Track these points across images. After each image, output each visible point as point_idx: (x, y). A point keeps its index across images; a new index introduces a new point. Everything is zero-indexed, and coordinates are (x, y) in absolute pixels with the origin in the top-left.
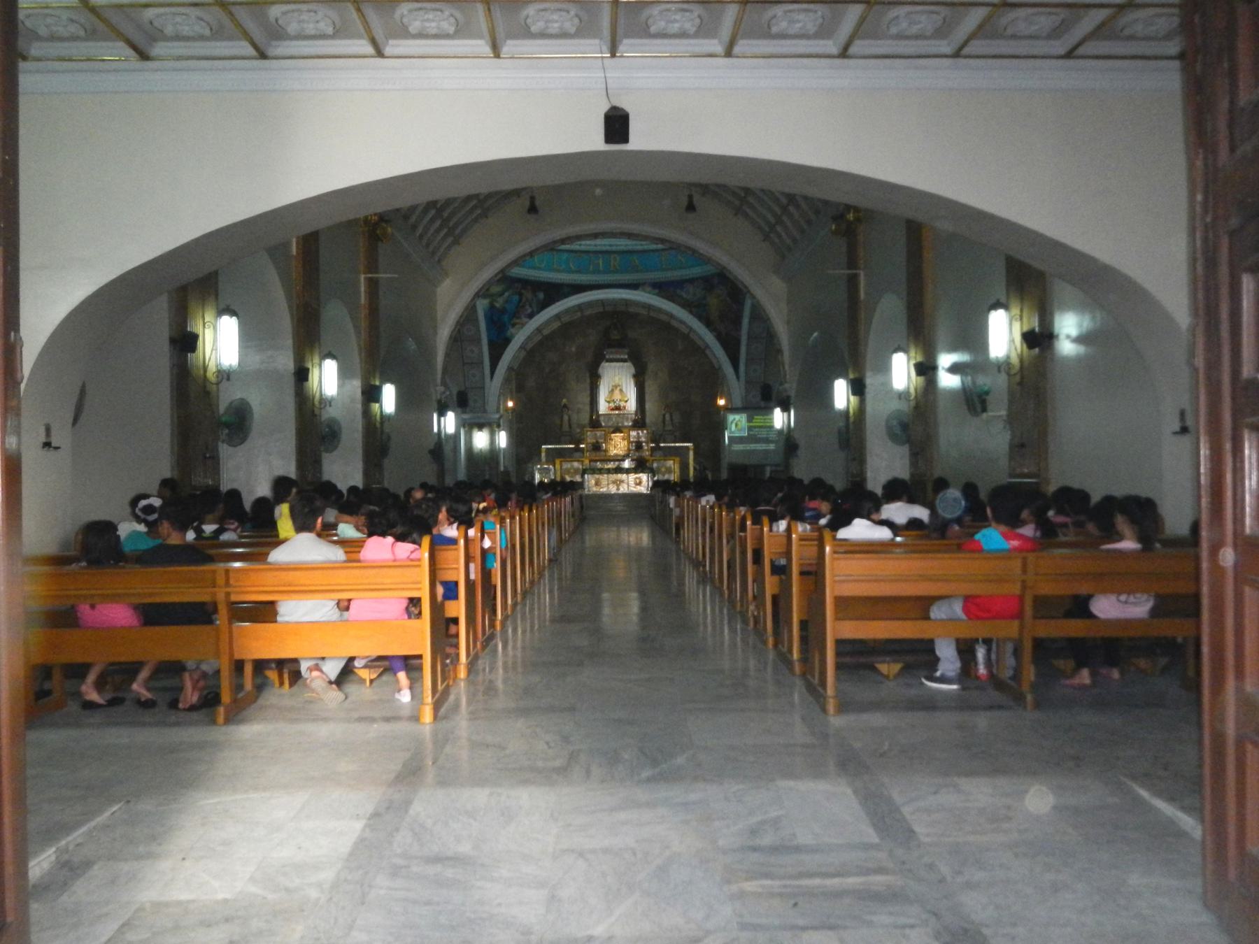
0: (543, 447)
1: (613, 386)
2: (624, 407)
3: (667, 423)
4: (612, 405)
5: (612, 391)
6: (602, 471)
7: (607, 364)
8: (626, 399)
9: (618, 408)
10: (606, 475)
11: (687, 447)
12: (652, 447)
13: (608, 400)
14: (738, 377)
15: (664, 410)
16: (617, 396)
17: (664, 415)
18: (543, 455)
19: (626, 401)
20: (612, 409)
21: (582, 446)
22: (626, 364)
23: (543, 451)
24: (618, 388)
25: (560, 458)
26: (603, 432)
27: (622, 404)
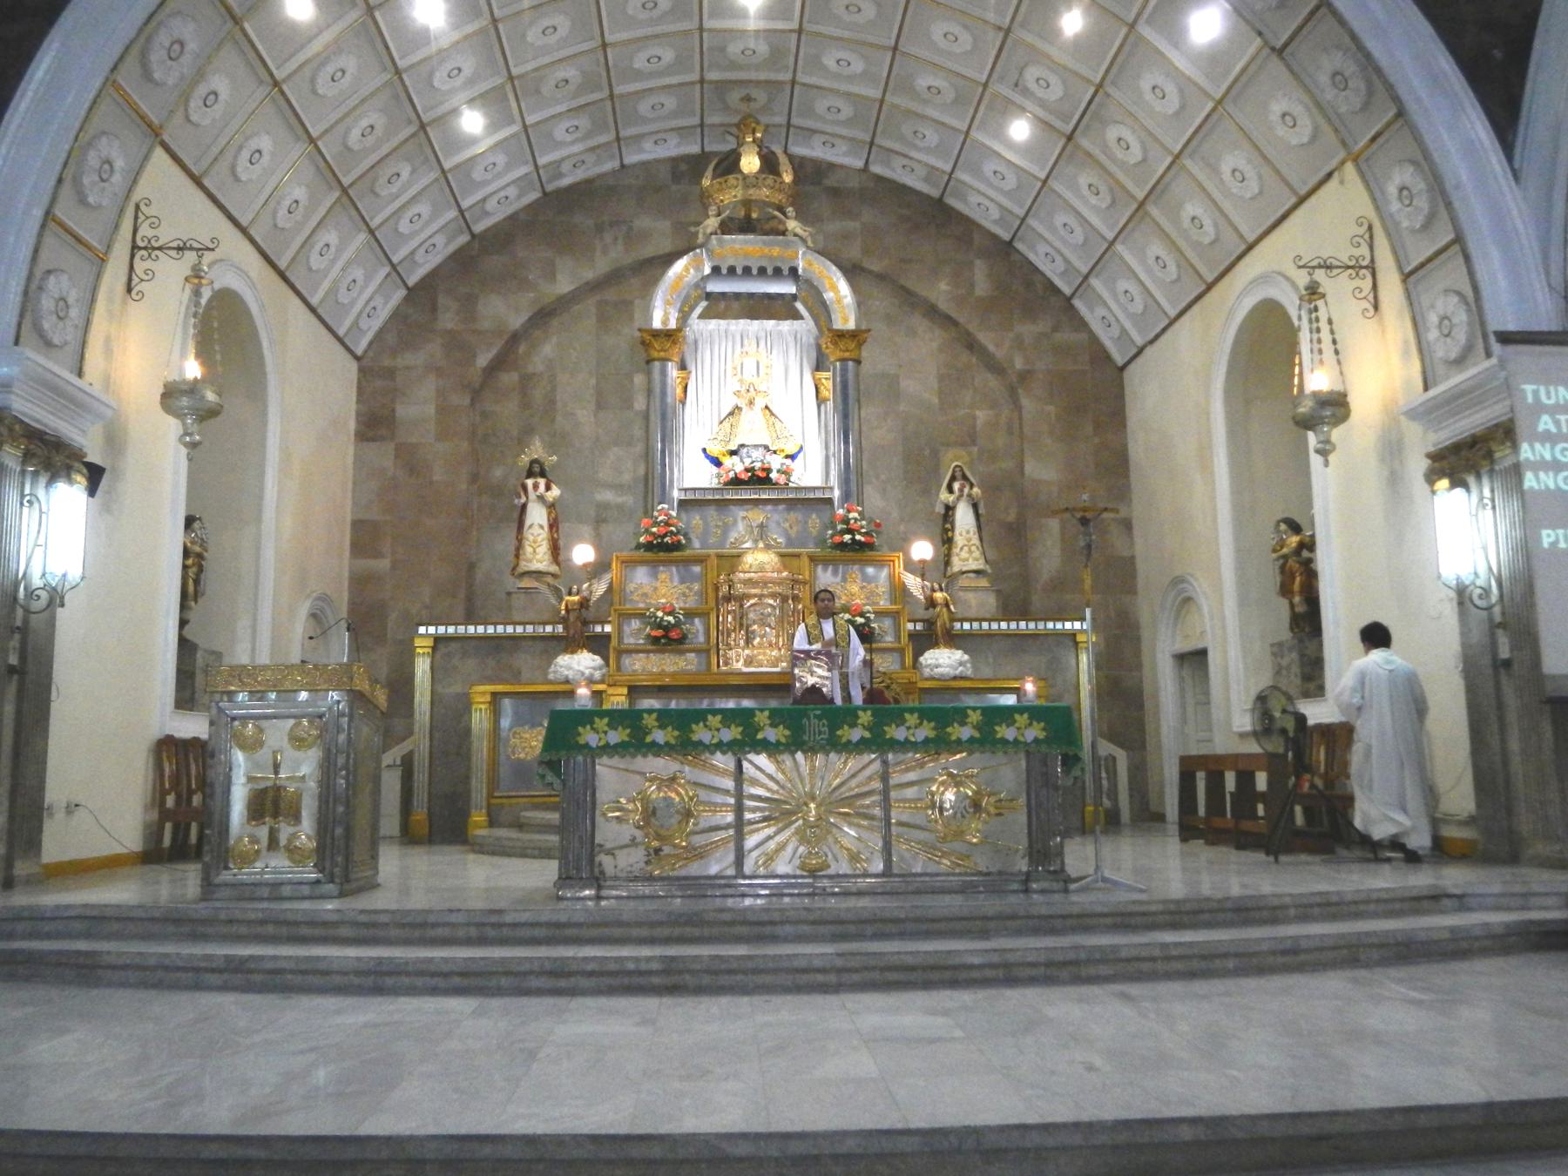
0: (422, 630)
1: (737, 393)
2: (786, 472)
3: (959, 540)
4: (736, 466)
5: (735, 411)
6: (701, 734)
7: (713, 324)
8: (792, 450)
9: (759, 479)
10: (723, 761)
11: (1073, 635)
12: (913, 636)
13: (715, 450)
14: (1516, 175)
15: (950, 490)
16: (751, 429)
17: (949, 509)
18: (422, 667)
19: (792, 457)
20: (736, 482)
21: (598, 629)
22: (786, 326)
23: (422, 645)
24: (760, 403)
25: (491, 681)
26: (697, 569)
27: (775, 462)
